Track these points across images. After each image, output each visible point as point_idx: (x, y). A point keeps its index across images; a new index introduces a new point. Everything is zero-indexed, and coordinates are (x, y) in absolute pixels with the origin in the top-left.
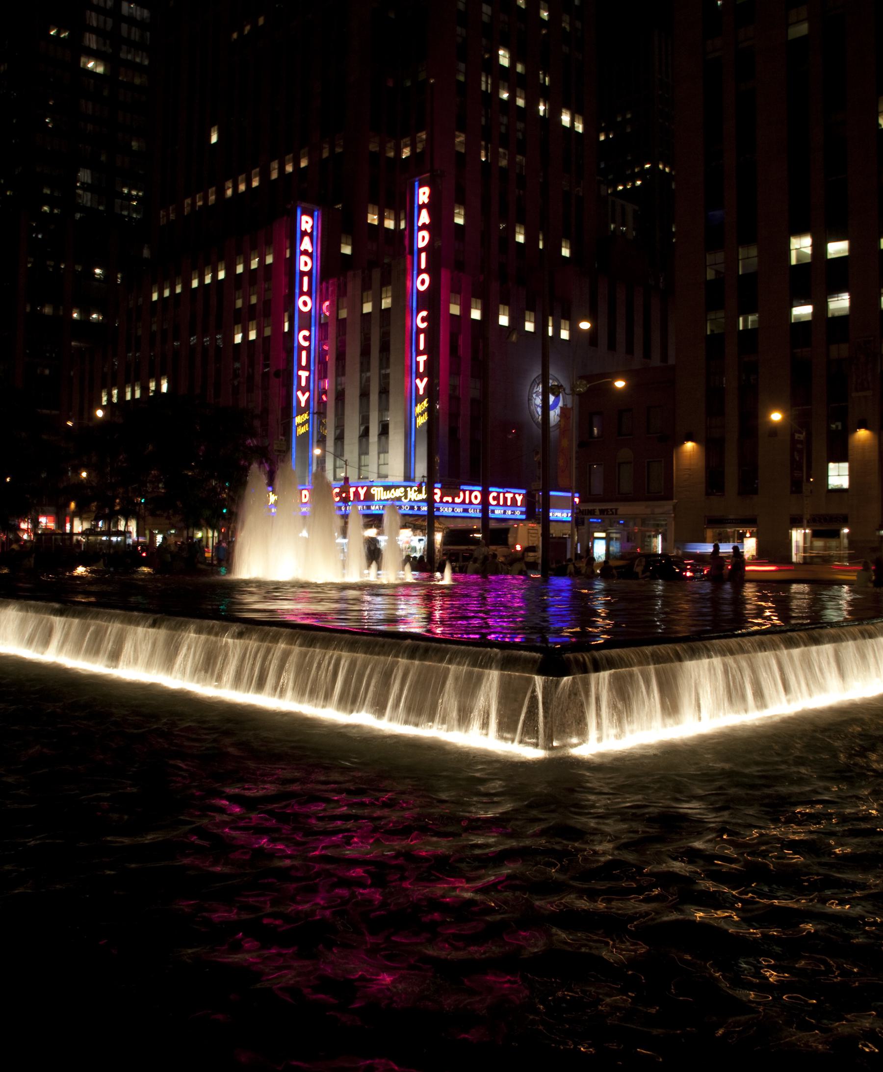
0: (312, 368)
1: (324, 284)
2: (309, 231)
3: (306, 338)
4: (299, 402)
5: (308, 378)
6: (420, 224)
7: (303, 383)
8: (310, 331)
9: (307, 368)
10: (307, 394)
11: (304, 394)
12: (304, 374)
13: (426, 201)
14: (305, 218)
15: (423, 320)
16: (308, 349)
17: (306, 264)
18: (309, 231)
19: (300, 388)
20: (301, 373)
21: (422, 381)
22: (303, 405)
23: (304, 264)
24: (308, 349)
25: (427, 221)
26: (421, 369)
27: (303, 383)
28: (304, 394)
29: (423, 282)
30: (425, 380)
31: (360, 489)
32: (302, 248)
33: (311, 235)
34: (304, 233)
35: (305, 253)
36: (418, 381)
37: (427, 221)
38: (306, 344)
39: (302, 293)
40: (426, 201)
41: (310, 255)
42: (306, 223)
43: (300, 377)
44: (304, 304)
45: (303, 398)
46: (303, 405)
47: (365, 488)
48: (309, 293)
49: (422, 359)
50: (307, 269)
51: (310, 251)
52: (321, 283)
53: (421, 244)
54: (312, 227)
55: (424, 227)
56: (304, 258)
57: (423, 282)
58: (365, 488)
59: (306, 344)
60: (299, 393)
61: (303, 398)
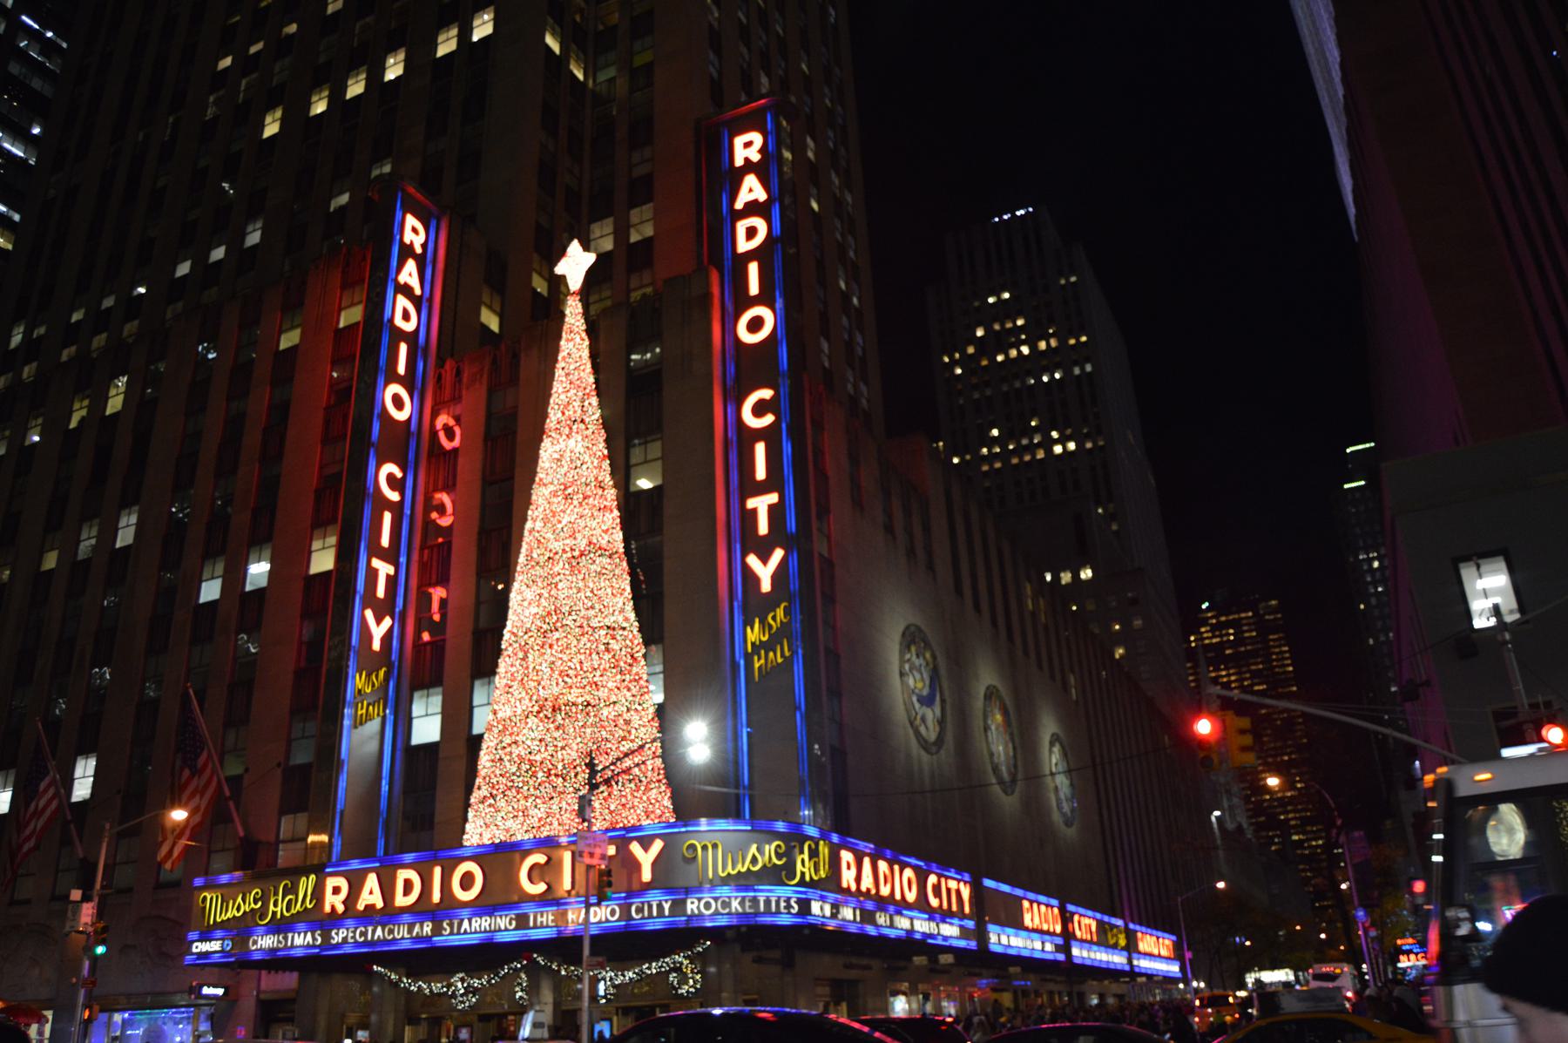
0: (403, 560)
1: (449, 364)
2: (419, 250)
3: (391, 478)
4: (367, 635)
5: (392, 581)
6: (739, 205)
7: (381, 593)
8: (403, 469)
9: (390, 556)
10: (387, 622)
11: (379, 621)
12: (384, 569)
13: (756, 157)
14: (411, 221)
15: (759, 410)
16: (397, 509)
17: (406, 316)
18: (419, 250)
19: (370, 600)
20: (376, 563)
21: (765, 560)
22: (376, 646)
23: (403, 315)
24: (397, 509)
25: (761, 195)
26: (763, 528)
27: (381, 593)
28: (379, 621)
29: (756, 324)
30: (779, 554)
31: (635, 848)
32: (403, 278)
33: (421, 261)
34: (407, 251)
35: (406, 290)
36: (753, 561)
37: (761, 195)
38: (394, 496)
39: (395, 378)
40: (756, 157)
41: (417, 301)
42: (413, 232)
43: (373, 574)
44: (397, 403)
45: (378, 631)
46: (376, 646)
47: (658, 845)
48: (408, 382)
49: (761, 504)
50: (409, 327)
51: (418, 291)
52: (441, 361)
53: (743, 246)
54: (424, 246)
55: (753, 208)
56: (402, 302)
57: (756, 324)
58: (658, 845)
59: (394, 496)
60: (369, 614)
61: (378, 631)
